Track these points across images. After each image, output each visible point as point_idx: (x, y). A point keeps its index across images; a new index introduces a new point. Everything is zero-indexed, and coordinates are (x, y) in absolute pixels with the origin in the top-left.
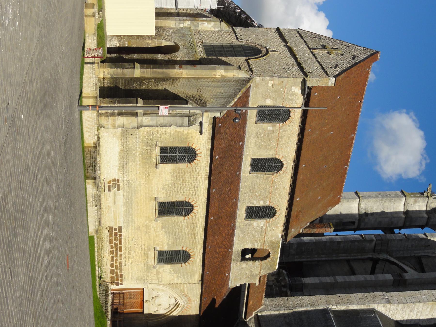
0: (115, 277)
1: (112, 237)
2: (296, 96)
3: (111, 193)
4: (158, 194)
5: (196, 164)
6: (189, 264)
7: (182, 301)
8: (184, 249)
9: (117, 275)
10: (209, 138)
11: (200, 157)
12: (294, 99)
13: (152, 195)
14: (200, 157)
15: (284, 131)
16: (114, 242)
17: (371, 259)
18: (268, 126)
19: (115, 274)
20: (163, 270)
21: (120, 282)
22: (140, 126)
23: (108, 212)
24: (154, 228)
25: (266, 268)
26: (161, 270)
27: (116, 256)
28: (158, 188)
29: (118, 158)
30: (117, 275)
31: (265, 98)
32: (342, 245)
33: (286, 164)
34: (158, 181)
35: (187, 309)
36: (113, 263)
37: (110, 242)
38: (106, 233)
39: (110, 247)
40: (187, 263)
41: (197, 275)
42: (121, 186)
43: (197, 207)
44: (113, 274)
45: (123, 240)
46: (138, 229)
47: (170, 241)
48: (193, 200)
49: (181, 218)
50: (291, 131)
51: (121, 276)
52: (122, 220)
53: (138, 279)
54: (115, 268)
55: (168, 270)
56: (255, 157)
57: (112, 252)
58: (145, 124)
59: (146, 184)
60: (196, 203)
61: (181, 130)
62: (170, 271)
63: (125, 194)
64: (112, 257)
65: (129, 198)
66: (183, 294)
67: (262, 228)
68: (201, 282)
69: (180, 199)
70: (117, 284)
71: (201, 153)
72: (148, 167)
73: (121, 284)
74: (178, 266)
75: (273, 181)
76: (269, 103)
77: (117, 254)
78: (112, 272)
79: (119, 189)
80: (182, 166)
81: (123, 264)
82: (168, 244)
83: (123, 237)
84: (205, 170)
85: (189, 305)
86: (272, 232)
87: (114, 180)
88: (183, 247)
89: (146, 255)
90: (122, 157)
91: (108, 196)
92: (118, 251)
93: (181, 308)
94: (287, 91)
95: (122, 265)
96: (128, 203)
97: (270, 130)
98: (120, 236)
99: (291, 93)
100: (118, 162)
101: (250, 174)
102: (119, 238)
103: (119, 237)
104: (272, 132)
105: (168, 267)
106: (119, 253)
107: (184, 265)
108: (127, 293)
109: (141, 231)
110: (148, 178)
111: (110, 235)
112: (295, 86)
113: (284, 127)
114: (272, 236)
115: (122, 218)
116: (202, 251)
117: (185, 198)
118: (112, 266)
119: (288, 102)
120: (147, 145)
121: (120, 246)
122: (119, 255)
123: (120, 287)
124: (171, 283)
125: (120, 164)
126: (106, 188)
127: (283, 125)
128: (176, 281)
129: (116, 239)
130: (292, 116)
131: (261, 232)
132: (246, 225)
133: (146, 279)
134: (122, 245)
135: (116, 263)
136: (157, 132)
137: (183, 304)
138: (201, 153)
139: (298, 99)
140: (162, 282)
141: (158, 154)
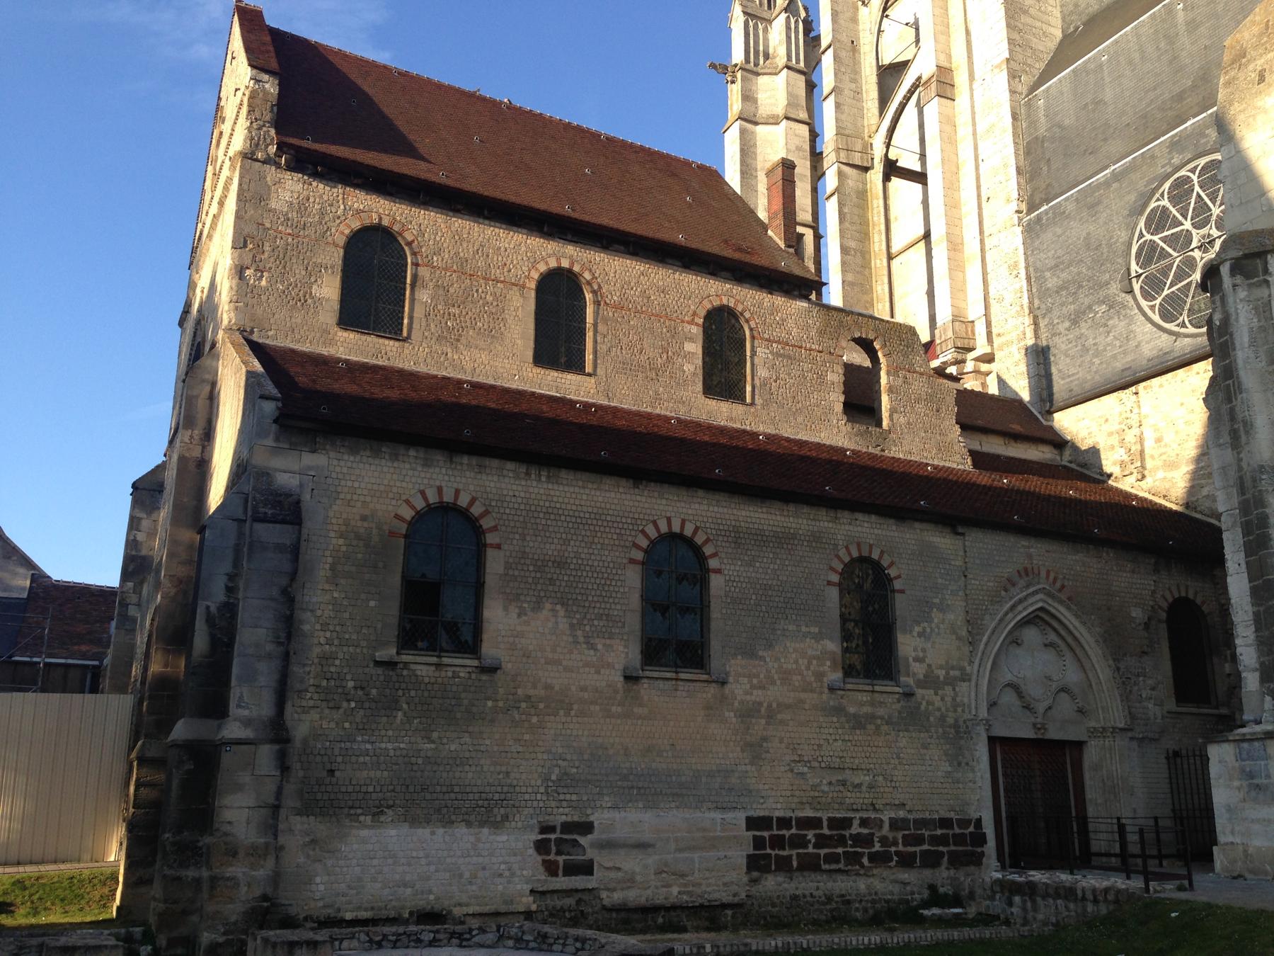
0: (953, 848)
1: (791, 856)
3: (601, 859)
4: (610, 666)
5: (486, 513)
6: (892, 564)
7: (1031, 600)
8: (835, 578)
9: (943, 840)
10: (377, 454)
11: (457, 492)
13: (616, 692)
14: (457, 492)
15: (438, 252)
16: (811, 850)
17: (886, 178)
18: (420, 302)
19: (941, 848)
20: (917, 660)
21: (971, 829)
22: (277, 731)
23: (683, 876)
24: (753, 687)
25: (906, 355)
26: (919, 669)
27: (866, 841)
28: (587, 665)
29: (441, 831)
30: (943, 840)
31: (304, 300)
32: (852, 244)
33: (558, 260)
34: (558, 662)
35: (1058, 585)
36: (897, 853)
37: (810, 865)
38: (772, 884)
39: (834, 866)
40: (892, 572)
41: (935, 539)
42: (569, 819)
43: (669, 520)
44: (943, 853)
45: (801, 814)
46: (756, 750)
47: (804, 629)
48: (643, 532)
49: (716, 582)
51: (945, 823)
52: (718, 815)
53: (958, 759)
54: (917, 849)
55: (919, 642)
56: (530, 354)
57: (854, 858)
58: (266, 709)
59: (567, 714)
60: (655, 523)
61: (330, 560)
62: (920, 635)
63: (607, 801)
64: (873, 858)
65: (625, 784)
66: (1003, 593)
67: (778, 355)
68: (960, 530)
69: (633, 579)
70: (980, 839)
71: (440, 489)
72: (490, 703)
73: (979, 821)
74: (901, 605)
75: (618, 307)
76: (329, 289)
77: (858, 840)
78: (931, 860)
79: (587, 828)
80: (495, 564)
81: (902, 814)
82: (818, 637)
83: (789, 814)
84: (517, 477)
85: (1043, 574)
86: (790, 323)
87: (541, 847)
88: (829, 583)
89: (859, 723)
90: (439, 811)
91: (613, 875)
92: (847, 833)
93: (1056, 605)
95: (905, 820)
96: (643, 788)
98: (784, 823)
99: (293, 215)
100: (461, 831)
101: (589, 375)
102: (794, 831)
103: (789, 827)
105: (907, 644)
106: (856, 829)
107: (897, 585)
108: (1008, 804)
109: (765, 739)
110: (541, 706)
111: (783, 865)
114: (807, 328)
115: (713, 815)
116: (845, 516)
117: (632, 561)
118: (906, 861)
120: (393, 705)
121: (825, 824)
122: (865, 831)
123: (989, 829)
124: (964, 633)
125: (469, 824)
126: (578, 882)
128: (956, 616)
129: (799, 842)
131: (789, 357)
132: (766, 404)
133: (956, 726)
134: (825, 816)
135: (895, 843)
136: (326, 658)
137: (1040, 596)
138: (440, 489)
140: (962, 669)
141: (434, 660)
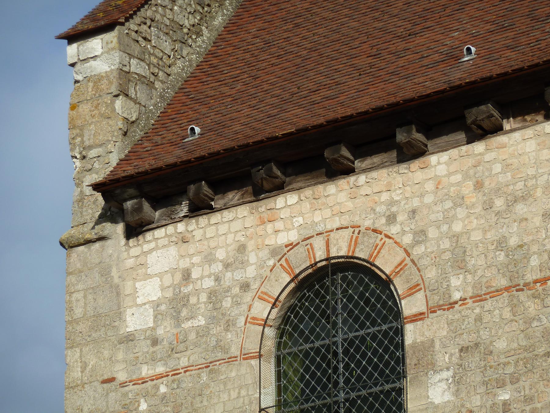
2: (187, 276)
12: (209, 283)
15: (460, 264)
50: (459, 201)
94: (154, 360)
97: (458, 382)
99: (165, 330)
104: (474, 360)
112: (120, 315)
113: (431, 274)
119: (229, 325)
127: (413, 290)
130: (340, 248)
139: (209, 259)
